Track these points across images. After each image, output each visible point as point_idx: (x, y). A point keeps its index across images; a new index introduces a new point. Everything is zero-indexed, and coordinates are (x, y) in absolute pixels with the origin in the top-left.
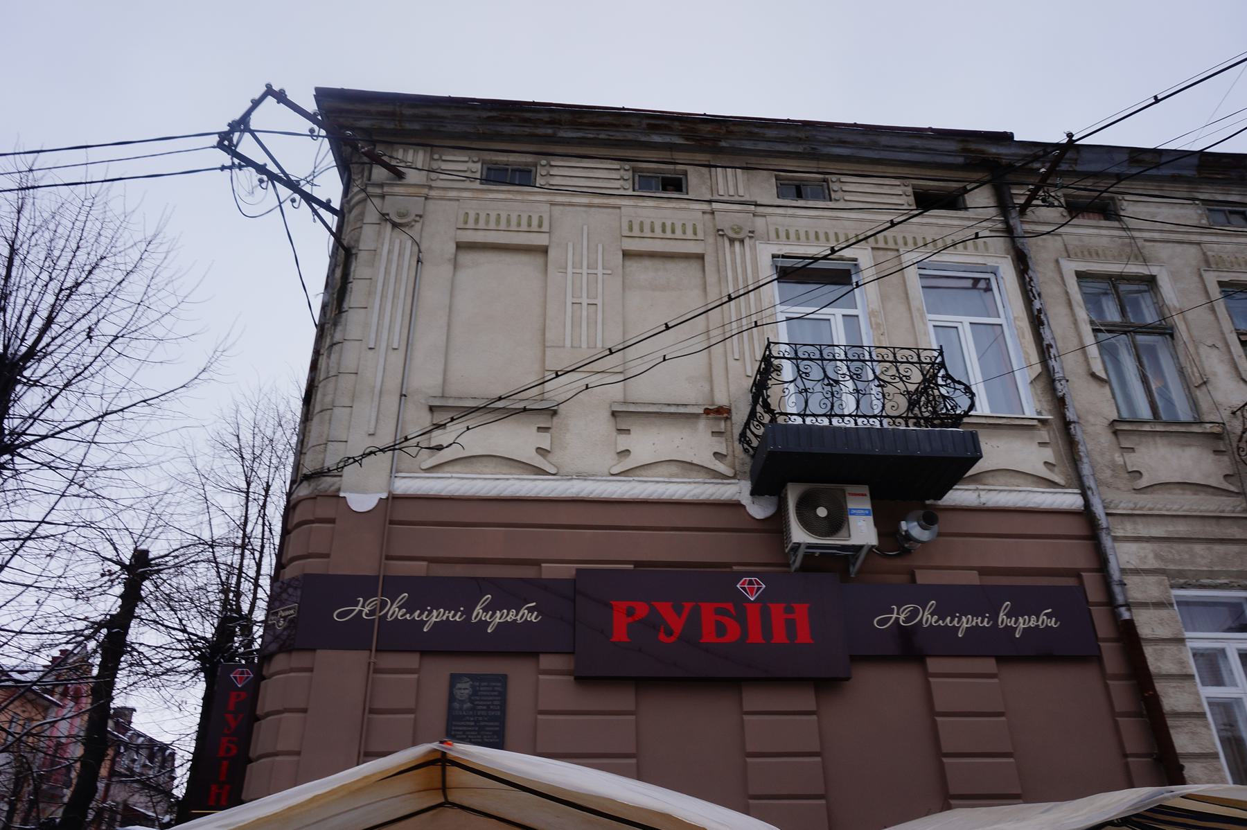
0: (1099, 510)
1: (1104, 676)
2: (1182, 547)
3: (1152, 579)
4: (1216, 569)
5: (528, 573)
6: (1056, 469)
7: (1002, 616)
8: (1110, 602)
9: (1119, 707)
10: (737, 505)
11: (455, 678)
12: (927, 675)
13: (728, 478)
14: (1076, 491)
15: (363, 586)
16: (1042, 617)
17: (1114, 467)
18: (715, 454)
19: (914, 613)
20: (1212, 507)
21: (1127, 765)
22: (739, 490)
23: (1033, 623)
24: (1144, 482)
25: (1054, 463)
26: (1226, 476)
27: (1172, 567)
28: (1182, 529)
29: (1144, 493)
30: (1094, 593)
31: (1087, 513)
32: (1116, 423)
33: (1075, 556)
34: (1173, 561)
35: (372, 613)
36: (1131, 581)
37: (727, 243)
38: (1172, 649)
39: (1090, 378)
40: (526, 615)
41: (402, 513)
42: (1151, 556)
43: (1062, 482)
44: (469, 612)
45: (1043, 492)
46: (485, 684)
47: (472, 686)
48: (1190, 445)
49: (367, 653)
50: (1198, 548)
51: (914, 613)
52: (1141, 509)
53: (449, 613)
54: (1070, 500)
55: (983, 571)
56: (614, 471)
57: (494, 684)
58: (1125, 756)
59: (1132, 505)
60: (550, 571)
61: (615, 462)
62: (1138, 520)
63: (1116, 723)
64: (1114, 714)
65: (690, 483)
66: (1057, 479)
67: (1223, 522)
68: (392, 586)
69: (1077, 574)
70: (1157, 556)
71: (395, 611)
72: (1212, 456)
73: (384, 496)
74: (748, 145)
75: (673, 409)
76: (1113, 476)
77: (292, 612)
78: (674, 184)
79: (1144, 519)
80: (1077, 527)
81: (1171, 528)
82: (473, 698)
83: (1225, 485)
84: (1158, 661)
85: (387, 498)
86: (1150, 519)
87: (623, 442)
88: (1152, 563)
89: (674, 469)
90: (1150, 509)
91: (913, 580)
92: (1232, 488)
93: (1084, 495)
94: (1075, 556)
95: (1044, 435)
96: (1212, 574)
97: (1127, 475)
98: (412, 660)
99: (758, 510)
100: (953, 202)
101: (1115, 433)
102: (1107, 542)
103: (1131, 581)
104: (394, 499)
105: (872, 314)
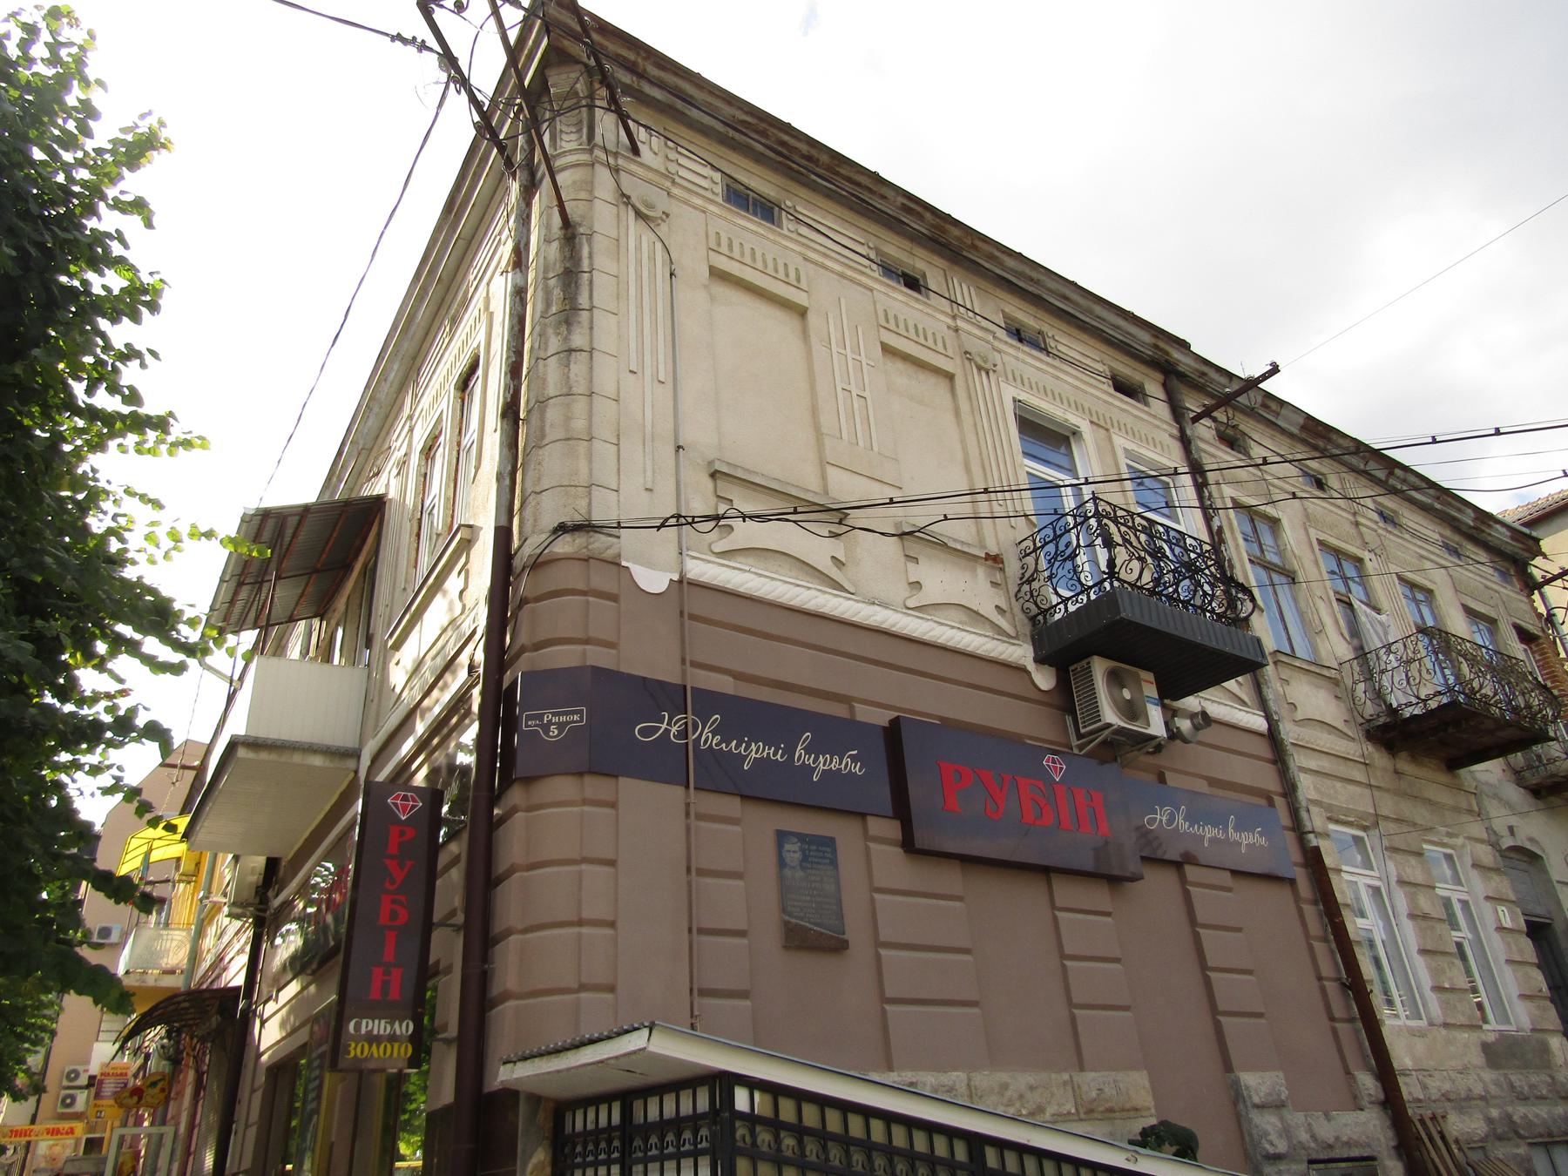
2: (1328, 782)
4: (1351, 806)
5: (839, 711)
7: (1231, 830)
10: (1022, 670)
11: (781, 836)
13: (1009, 636)
15: (670, 697)
18: (997, 606)
20: (1343, 749)
22: (1022, 653)
24: (1299, 715)
27: (1326, 800)
29: (1304, 727)
31: (1272, 736)
32: (1279, 654)
35: (683, 734)
40: (847, 764)
41: (698, 604)
42: (1312, 787)
43: (1249, 704)
44: (790, 751)
45: (1240, 710)
46: (815, 848)
47: (803, 850)
48: (1321, 688)
49: (677, 792)
50: (1339, 785)
52: (1302, 740)
53: (769, 749)
56: (911, 604)
57: (824, 849)
60: (865, 714)
61: (907, 594)
65: (981, 635)
67: (1348, 762)
68: (708, 702)
71: (707, 737)
72: (1334, 702)
73: (676, 577)
75: (959, 547)
77: (576, 717)
80: (1263, 749)
81: (1320, 763)
82: (804, 864)
83: (1345, 730)
85: (680, 582)
87: (916, 572)
89: (962, 616)
91: (1162, 779)
92: (1350, 733)
96: (1348, 812)
97: (1287, 706)
98: (732, 806)
99: (1044, 680)
104: (683, 585)
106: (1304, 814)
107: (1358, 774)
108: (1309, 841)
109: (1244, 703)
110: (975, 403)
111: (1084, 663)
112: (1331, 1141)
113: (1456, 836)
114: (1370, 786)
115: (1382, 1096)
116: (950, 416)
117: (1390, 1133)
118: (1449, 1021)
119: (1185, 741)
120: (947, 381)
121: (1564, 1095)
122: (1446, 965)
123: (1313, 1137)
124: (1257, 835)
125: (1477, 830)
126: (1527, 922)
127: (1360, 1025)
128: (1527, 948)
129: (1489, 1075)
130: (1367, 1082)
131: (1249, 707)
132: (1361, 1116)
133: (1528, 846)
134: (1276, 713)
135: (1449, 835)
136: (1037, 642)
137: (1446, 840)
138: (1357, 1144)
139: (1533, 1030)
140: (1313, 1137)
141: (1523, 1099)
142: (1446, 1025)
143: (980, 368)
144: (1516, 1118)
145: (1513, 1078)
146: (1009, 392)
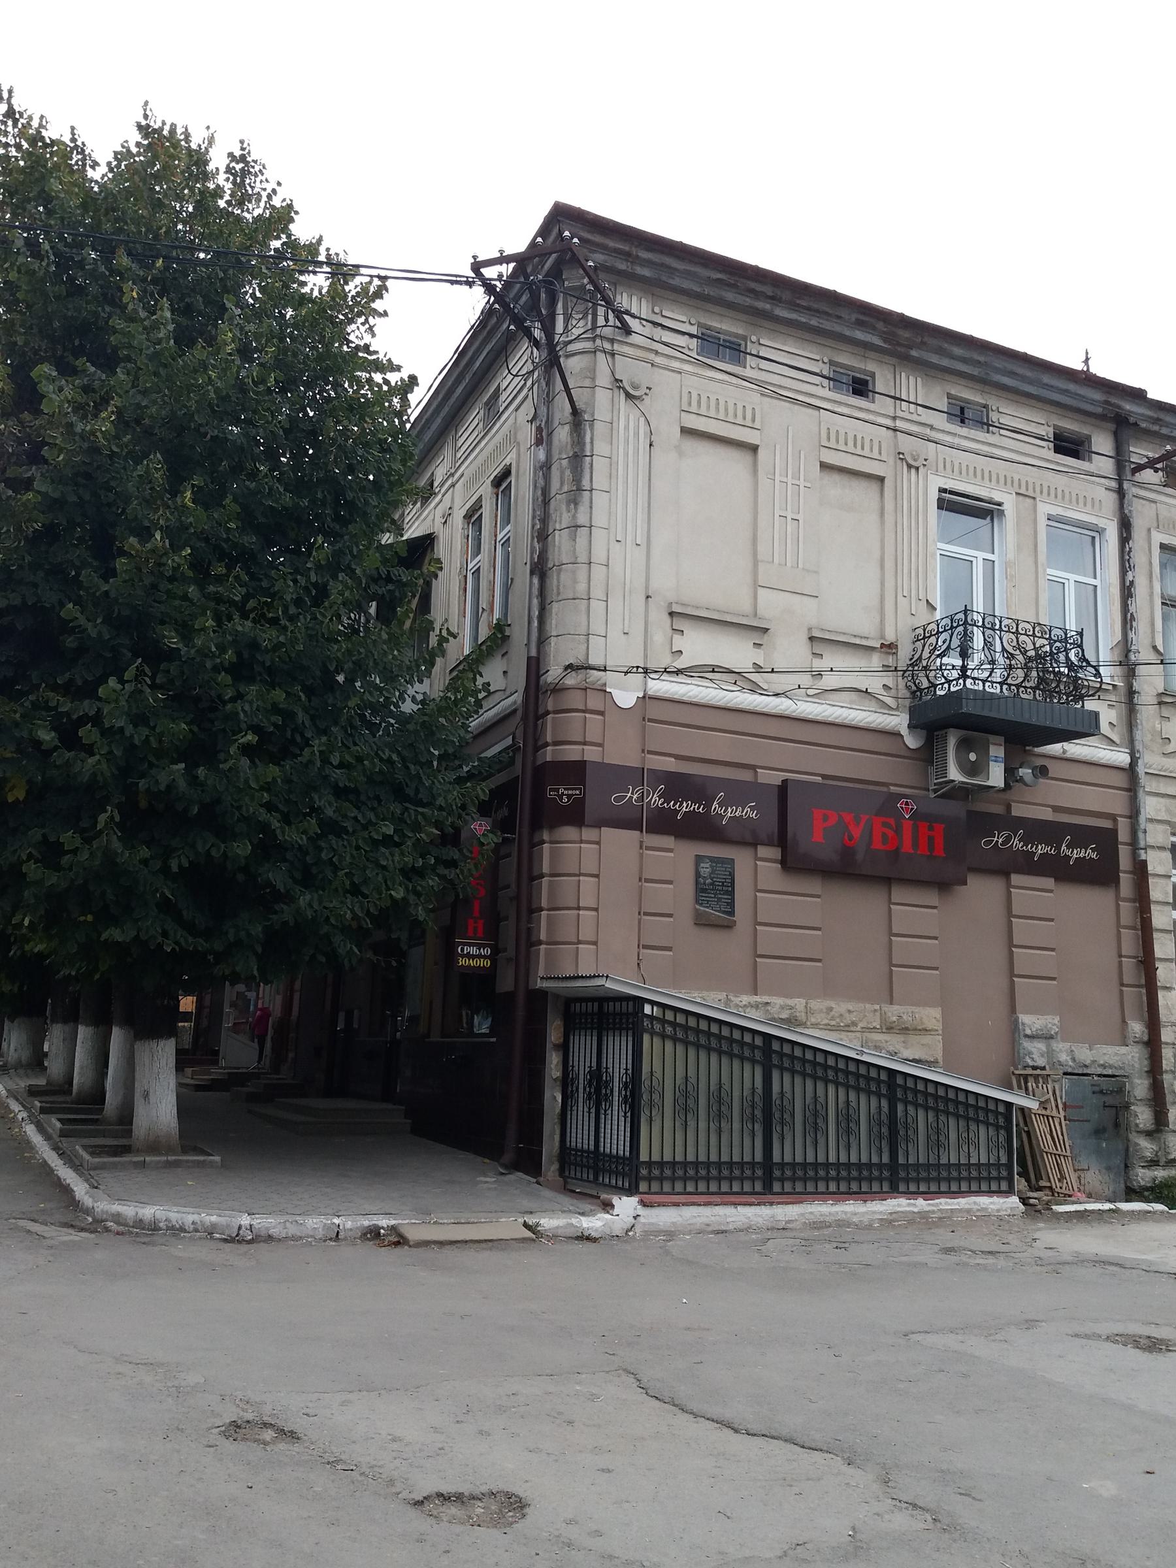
0: (1141, 769)
1: (1118, 897)
3: (1160, 827)
6: (1116, 729)
7: (1064, 847)
8: (1134, 844)
9: (1123, 922)
12: (1009, 885)
13: (890, 708)
14: (1127, 750)
16: (1089, 851)
19: (1008, 839)
21: (1120, 963)
22: (899, 721)
23: (1082, 855)
30: (1123, 835)
33: (1115, 803)
36: (1150, 827)
37: (905, 467)
38: (1162, 881)
42: (1164, 809)
43: (1118, 742)
51: (1008, 839)
54: (1122, 758)
55: (1056, 809)
58: (1120, 956)
59: (1160, 767)
62: (1161, 779)
63: (1119, 933)
64: (1118, 925)
66: (1115, 738)
69: (1113, 818)
70: (1168, 811)
74: (934, 359)
76: (1151, 740)
78: (861, 388)
80: (1120, 780)
88: (1163, 816)
90: (1171, 772)
93: (1132, 754)
94: (1115, 803)
99: (912, 742)
102: (1141, 794)
103: (1150, 827)
105: (1007, 565)
106: (1141, 835)
108: (1139, 856)
109: (1111, 741)
110: (899, 502)
111: (944, 732)
112: (1088, 1062)
115: (1146, 1038)
116: (874, 517)
117: (1146, 1062)
119: (1026, 785)
120: (879, 483)
123: (1074, 1060)
124: (1089, 851)
127: (1144, 991)
130: (1137, 1028)
131: (1117, 745)
132: (1124, 1050)
134: (1138, 751)
136: (912, 712)
138: (1111, 1067)
140: (1074, 1060)
143: (910, 466)
146: (936, 482)
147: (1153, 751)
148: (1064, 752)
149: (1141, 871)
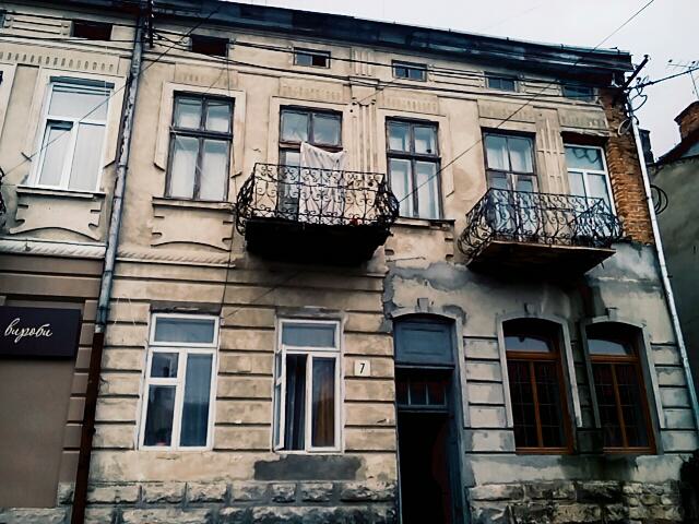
17: (143, 230)
25: (96, 224)
26: (224, 240)
28: (176, 273)
34: (158, 295)
39: (153, 167)
69: (82, 300)
70: (149, 291)
79: (149, 266)
84: (112, 359)
86: (153, 266)
95: (97, 205)
96: (185, 304)
100: (103, 33)
101: (154, 206)
107: (216, 276)
113: (337, 311)
114: (226, 283)
118: (219, 447)
121: (344, 498)
122: (248, 408)
125: (376, 303)
126: (396, 369)
128: (388, 390)
129: (252, 483)
133: (438, 311)
135: (322, 311)
137: (322, 315)
139: (346, 451)
141: (282, 500)
142: (215, 450)
144: (256, 516)
145: (275, 487)
147: (140, 244)
148: (28, 249)
149: (99, 344)
